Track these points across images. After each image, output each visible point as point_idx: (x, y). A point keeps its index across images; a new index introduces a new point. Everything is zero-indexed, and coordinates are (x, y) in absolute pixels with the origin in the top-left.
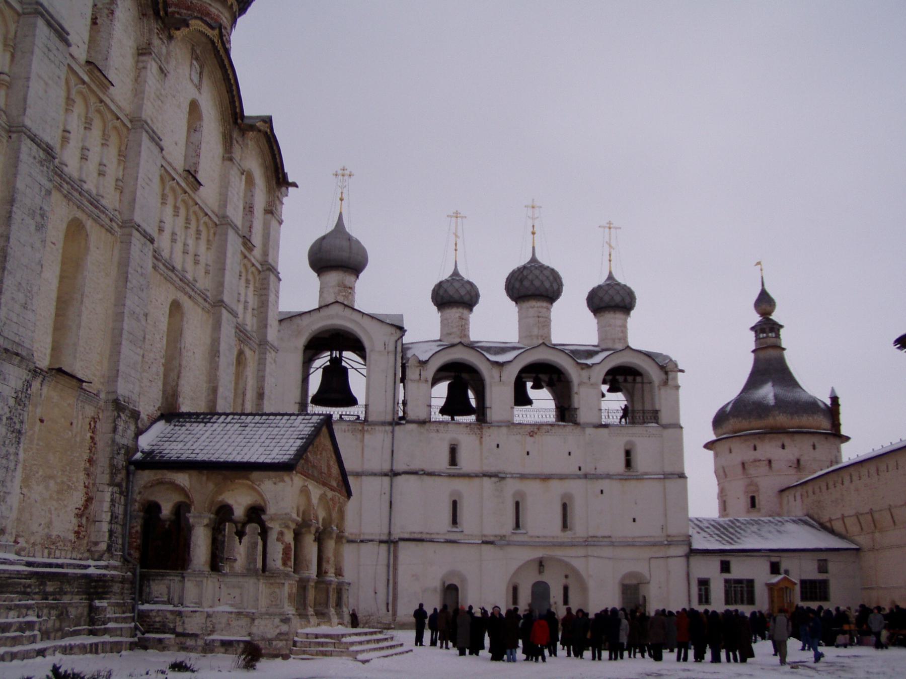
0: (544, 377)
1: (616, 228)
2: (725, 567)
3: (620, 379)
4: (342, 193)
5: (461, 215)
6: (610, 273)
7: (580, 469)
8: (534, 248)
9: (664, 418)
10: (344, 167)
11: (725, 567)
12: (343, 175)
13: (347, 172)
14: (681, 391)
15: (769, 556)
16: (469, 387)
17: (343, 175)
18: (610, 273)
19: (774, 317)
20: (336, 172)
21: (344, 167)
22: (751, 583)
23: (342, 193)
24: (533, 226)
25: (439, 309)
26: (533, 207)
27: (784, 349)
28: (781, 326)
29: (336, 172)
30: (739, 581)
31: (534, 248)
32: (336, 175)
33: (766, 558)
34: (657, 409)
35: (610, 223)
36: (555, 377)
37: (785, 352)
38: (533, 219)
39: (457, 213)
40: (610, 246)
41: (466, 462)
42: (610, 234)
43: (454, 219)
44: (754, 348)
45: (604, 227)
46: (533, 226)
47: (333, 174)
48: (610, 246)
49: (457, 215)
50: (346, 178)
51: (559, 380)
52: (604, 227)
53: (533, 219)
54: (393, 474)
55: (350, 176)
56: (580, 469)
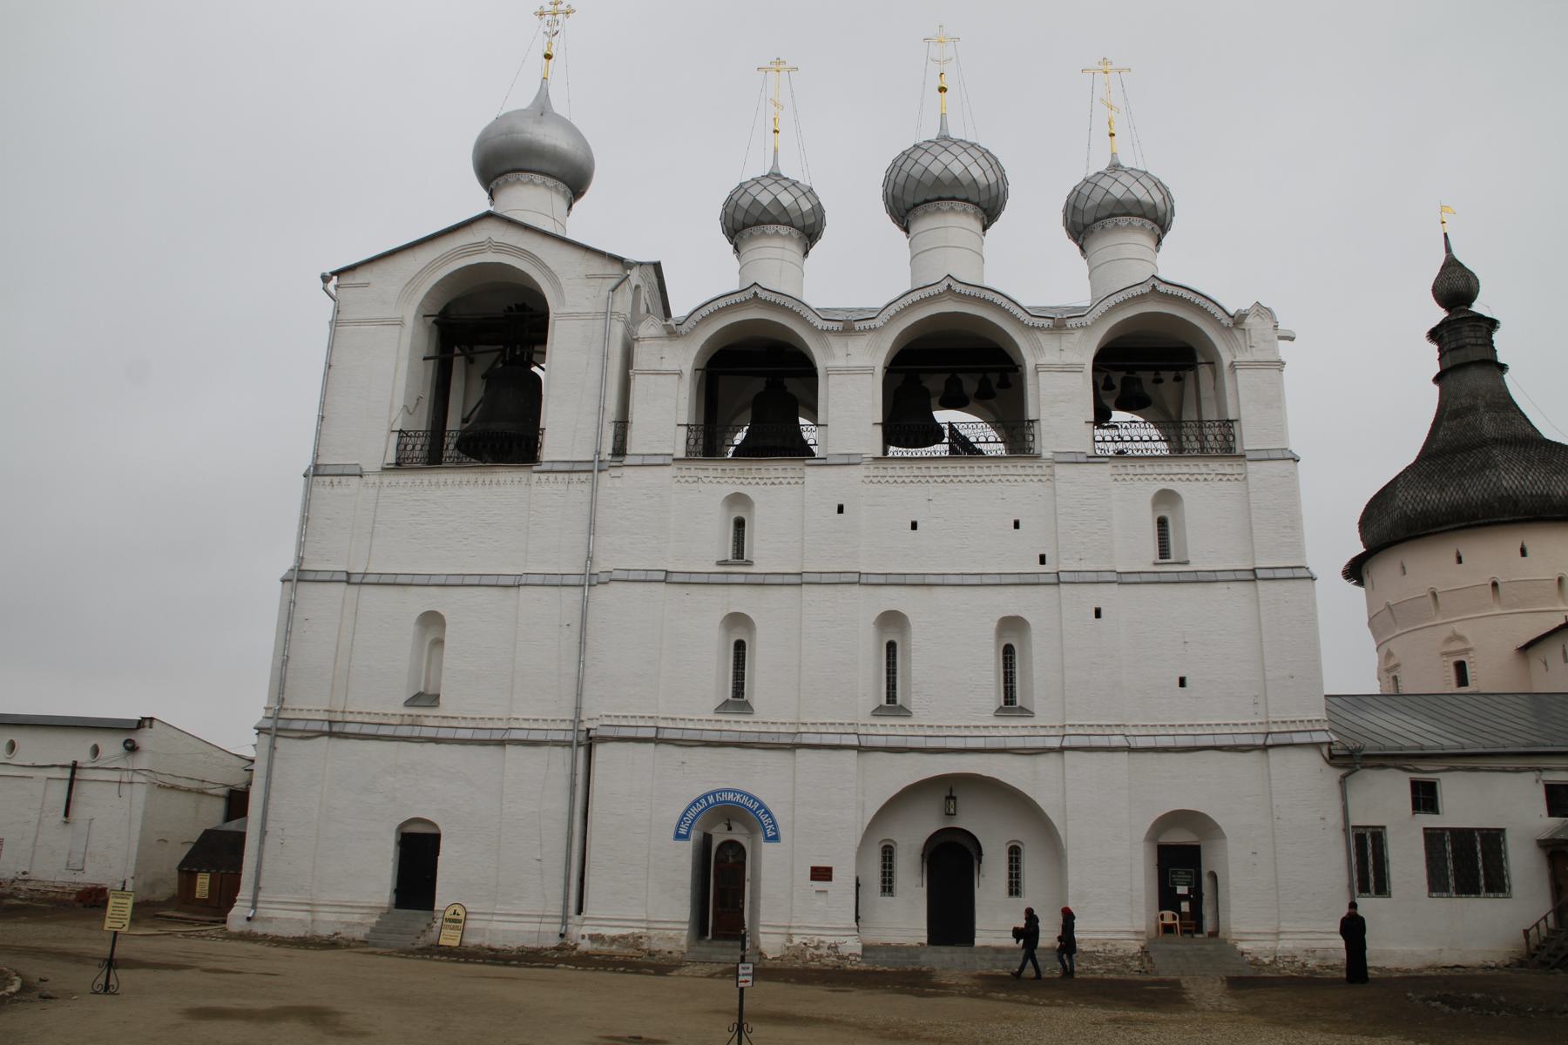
0: (970, 385)
2: (1425, 797)
3: (1146, 377)
6: (1113, 155)
7: (1042, 560)
9: (1249, 438)
11: (1425, 797)
13: (562, 7)
15: (1540, 770)
16: (801, 409)
19: (1478, 307)
22: (1494, 838)
27: (1503, 368)
28: (1493, 324)
30: (1463, 837)
33: (1532, 776)
36: (994, 378)
37: (1506, 377)
41: (765, 553)
44: (1438, 370)
47: (535, 14)
50: (560, 17)
51: (1005, 384)
54: (590, 580)
55: (567, 13)
56: (1042, 560)
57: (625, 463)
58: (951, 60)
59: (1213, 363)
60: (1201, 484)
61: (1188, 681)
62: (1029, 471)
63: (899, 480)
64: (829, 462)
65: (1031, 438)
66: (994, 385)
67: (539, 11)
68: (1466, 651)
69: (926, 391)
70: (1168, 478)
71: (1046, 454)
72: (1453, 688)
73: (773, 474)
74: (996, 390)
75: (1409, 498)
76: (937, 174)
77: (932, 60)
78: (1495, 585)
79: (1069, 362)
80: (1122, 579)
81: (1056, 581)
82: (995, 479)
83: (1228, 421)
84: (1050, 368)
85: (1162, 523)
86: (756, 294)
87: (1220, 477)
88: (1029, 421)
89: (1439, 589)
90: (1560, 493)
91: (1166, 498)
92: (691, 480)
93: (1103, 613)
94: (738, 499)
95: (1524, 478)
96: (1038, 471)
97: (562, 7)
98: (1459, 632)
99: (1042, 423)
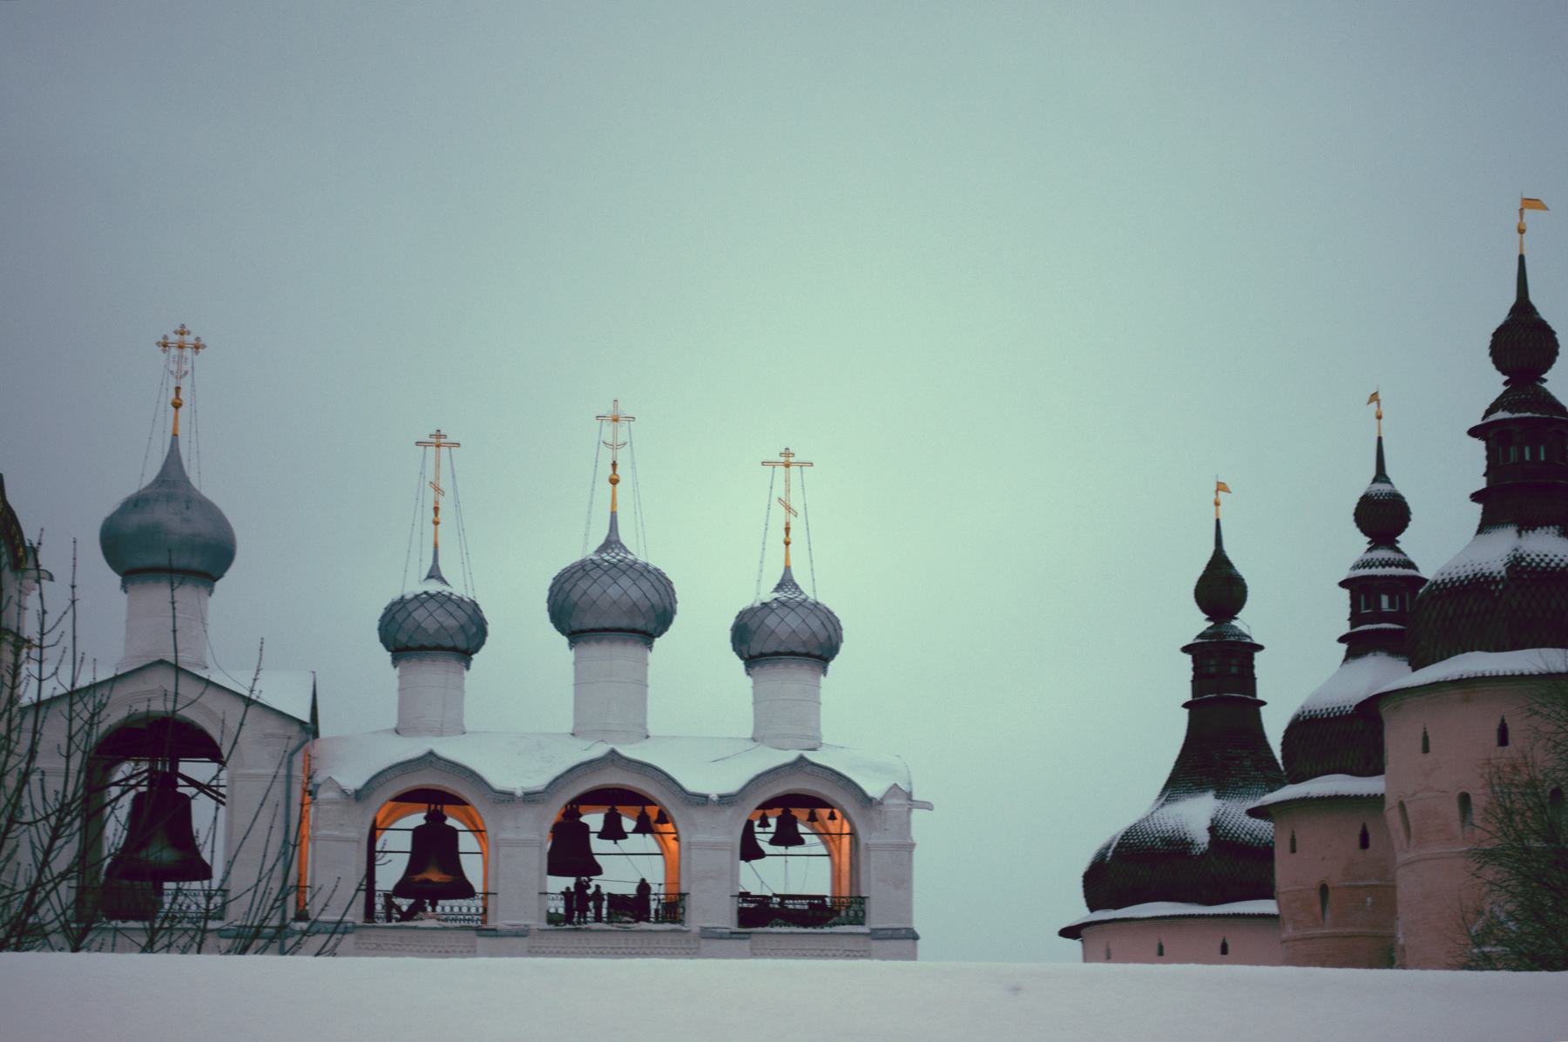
1: (801, 465)
4: (178, 389)
5: (449, 439)
6: (787, 569)
8: (614, 516)
10: (183, 326)
12: (181, 347)
13: (190, 339)
14: (916, 852)
17: (181, 347)
18: (787, 569)
20: (165, 337)
21: (183, 326)
23: (178, 389)
24: (614, 465)
25: (395, 661)
26: (616, 420)
29: (165, 337)
31: (614, 516)
32: (165, 345)
34: (863, 895)
35: (787, 453)
36: (652, 812)
38: (614, 447)
39: (439, 435)
40: (788, 509)
42: (787, 481)
43: (431, 450)
45: (774, 464)
46: (614, 465)
48: (788, 509)
49: (438, 440)
50: (188, 352)
52: (774, 464)
53: (614, 447)
58: (625, 444)
65: (681, 911)
67: (162, 341)
69: (586, 827)
77: (605, 443)
83: (860, 897)
87: (847, 952)
97: (190, 339)
99: (692, 893)
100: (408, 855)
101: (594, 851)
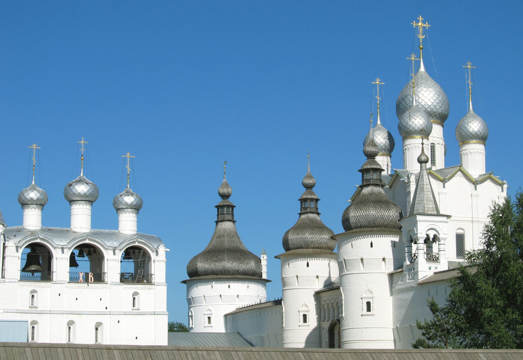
0: (86, 250)
3: (131, 251)
36: (92, 250)
57: (6, 281)
59: (149, 257)
60: (144, 290)
61: (138, 338)
62: (105, 286)
63: (74, 287)
64: (57, 283)
66: (92, 252)
68: (211, 314)
70: (136, 289)
71: (109, 282)
72: (207, 324)
73: (43, 285)
74: (92, 254)
75: (201, 266)
76: (79, 192)
78: (220, 296)
79: (115, 259)
80: (125, 314)
81: (110, 314)
82: (96, 288)
84: (111, 260)
85: (134, 299)
86: (39, 236)
87: (148, 289)
88: (104, 273)
89: (206, 295)
90: (241, 270)
91: (136, 294)
92: (22, 286)
93: (120, 322)
94: (34, 291)
95: (232, 264)
96: (107, 286)
98: (210, 308)
100: (26, 260)
101: (76, 260)
